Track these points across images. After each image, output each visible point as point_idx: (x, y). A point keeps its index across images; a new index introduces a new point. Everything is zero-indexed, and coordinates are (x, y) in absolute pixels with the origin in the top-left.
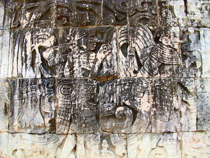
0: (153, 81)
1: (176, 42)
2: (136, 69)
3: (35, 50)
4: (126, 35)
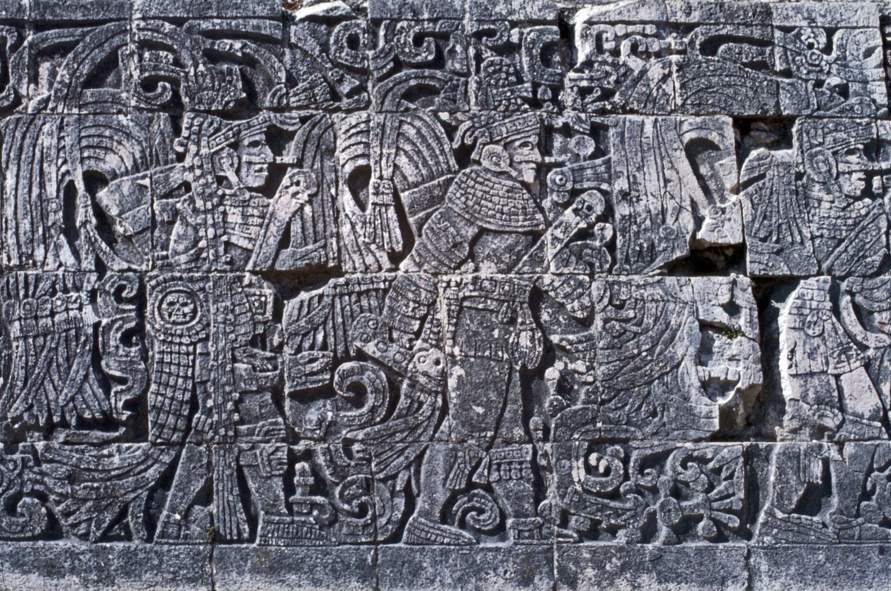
0: (453, 284)
1: (527, 162)
2: (399, 248)
3: (72, 183)
4: (364, 140)
